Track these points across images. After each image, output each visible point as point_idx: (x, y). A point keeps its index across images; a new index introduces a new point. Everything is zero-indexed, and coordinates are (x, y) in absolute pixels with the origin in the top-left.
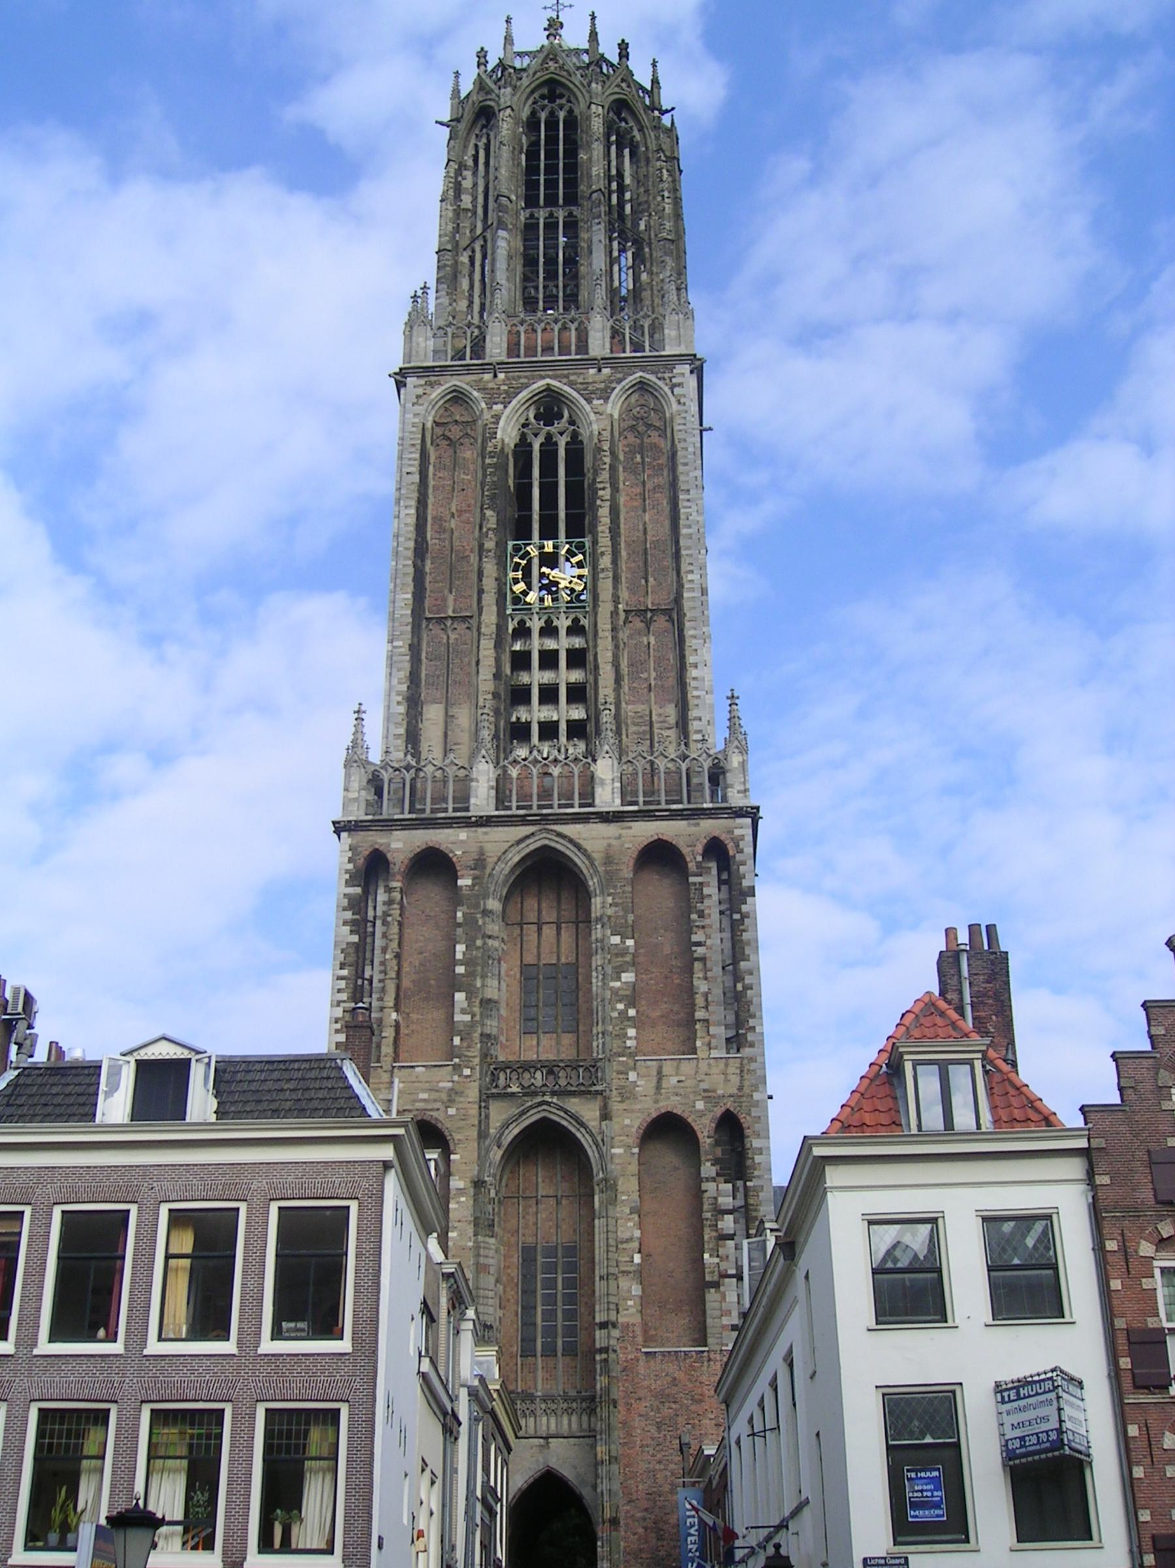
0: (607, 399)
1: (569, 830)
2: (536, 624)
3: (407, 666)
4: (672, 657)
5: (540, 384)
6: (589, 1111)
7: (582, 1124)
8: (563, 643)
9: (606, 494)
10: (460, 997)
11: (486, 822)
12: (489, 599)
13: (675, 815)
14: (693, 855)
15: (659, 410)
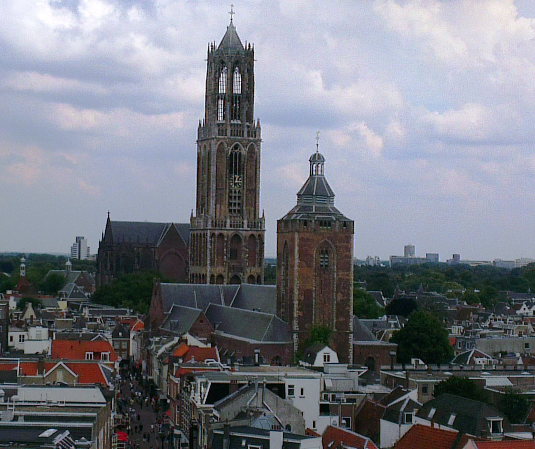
0: (246, 147)
1: (241, 232)
2: (233, 191)
3: (215, 199)
4: (254, 199)
5: (236, 143)
6: (242, 274)
7: (241, 276)
8: (237, 195)
9: (246, 168)
10: (225, 257)
11: (229, 230)
12: (228, 187)
13: (254, 230)
14: (257, 237)
15: (254, 149)
